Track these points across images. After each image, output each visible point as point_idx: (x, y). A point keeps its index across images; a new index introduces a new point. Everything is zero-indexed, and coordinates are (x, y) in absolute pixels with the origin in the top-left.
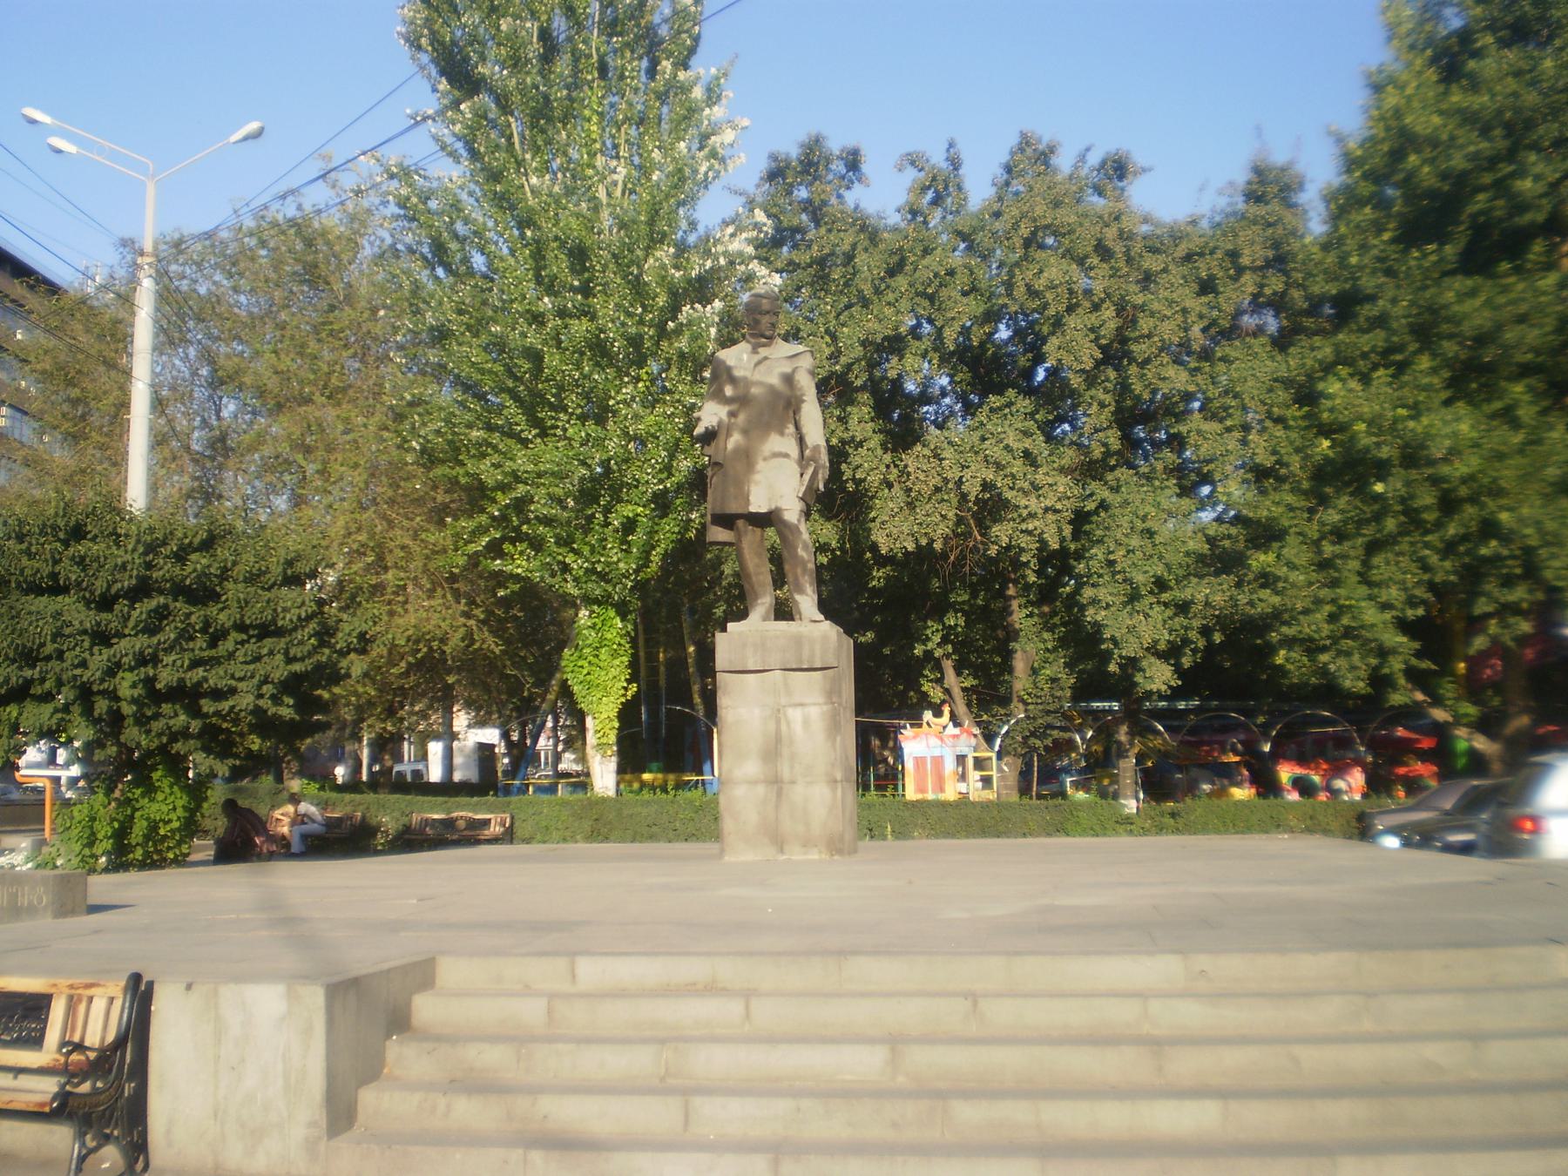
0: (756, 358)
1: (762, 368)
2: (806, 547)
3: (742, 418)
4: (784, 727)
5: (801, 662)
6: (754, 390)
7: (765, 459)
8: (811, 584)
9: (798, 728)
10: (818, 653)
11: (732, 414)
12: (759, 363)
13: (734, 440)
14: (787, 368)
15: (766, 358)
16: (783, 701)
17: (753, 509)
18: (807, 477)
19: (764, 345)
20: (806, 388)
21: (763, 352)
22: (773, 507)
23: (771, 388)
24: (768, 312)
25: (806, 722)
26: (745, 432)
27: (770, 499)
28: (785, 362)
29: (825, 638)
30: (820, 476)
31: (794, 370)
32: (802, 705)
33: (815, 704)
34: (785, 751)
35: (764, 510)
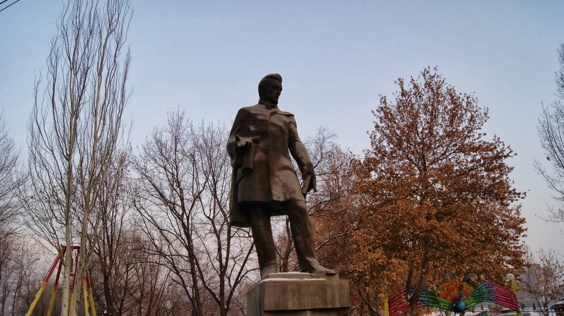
0: (270, 111)
3: (261, 145)
5: (326, 302)
6: (272, 129)
10: (337, 297)
11: (256, 141)
12: (272, 114)
13: (260, 155)
14: (287, 120)
15: (275, 113)
17: (275, 198)
18: (308, 182)
21: (273, 110)
22: (288, 197)
23: (280, 127)
26: (266, 152)
27: (284, 194)
31: (290, 122)
35: (282, 199)
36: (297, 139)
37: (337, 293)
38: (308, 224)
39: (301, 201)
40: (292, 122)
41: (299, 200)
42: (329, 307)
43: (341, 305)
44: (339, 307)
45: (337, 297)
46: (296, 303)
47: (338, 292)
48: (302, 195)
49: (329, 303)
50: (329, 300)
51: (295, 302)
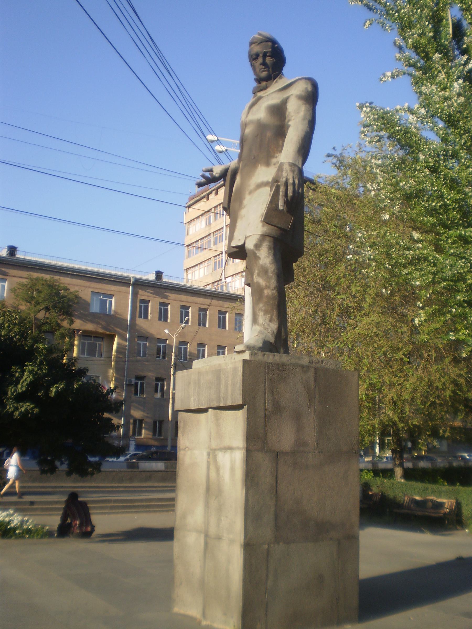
1: (255, 108)
2: (264, 271)
4: (213, 474)
7: (250, 193)
8: (266, 312)
9: (226, 475)
10: (230, 388)
15: (260, 98)
16: (214, 446)
19: (265, 88)
20: (292, 114)
24: (257, 56)
25: (232, 469)
28: (275, 95)
29: (235, 369)
30: (281, 194)
32: (230, 449)
33: (238, 448)
34: (214, 503)
36: (290, 123)
37: (230, 382)
38: (256, 272)
39: (250, 237)
40: (292, 95)
41: (249, 236)
42: (222, 405)
43: (232, 402)
44: (230, 405)
45: (230, 388)
46: (196, 399)
47: (231, 381)
48: (261, 224)
49: (222, 399)
50: (222, 395)
51: (195, 398)
